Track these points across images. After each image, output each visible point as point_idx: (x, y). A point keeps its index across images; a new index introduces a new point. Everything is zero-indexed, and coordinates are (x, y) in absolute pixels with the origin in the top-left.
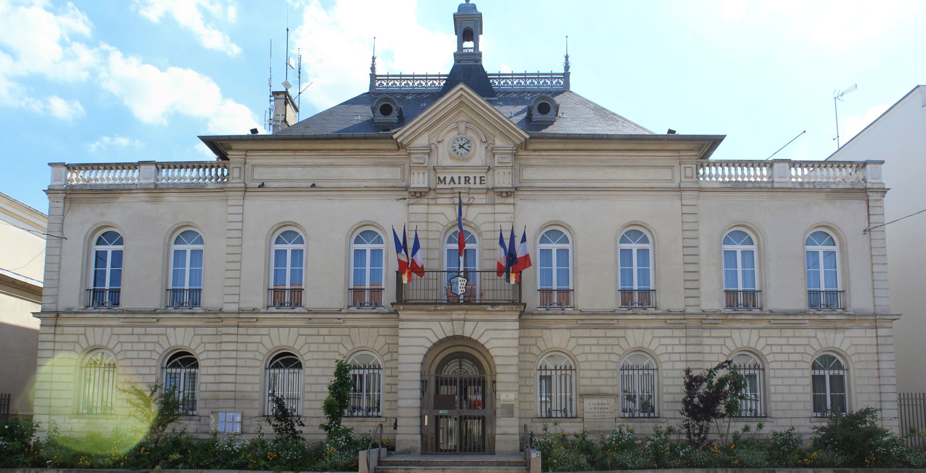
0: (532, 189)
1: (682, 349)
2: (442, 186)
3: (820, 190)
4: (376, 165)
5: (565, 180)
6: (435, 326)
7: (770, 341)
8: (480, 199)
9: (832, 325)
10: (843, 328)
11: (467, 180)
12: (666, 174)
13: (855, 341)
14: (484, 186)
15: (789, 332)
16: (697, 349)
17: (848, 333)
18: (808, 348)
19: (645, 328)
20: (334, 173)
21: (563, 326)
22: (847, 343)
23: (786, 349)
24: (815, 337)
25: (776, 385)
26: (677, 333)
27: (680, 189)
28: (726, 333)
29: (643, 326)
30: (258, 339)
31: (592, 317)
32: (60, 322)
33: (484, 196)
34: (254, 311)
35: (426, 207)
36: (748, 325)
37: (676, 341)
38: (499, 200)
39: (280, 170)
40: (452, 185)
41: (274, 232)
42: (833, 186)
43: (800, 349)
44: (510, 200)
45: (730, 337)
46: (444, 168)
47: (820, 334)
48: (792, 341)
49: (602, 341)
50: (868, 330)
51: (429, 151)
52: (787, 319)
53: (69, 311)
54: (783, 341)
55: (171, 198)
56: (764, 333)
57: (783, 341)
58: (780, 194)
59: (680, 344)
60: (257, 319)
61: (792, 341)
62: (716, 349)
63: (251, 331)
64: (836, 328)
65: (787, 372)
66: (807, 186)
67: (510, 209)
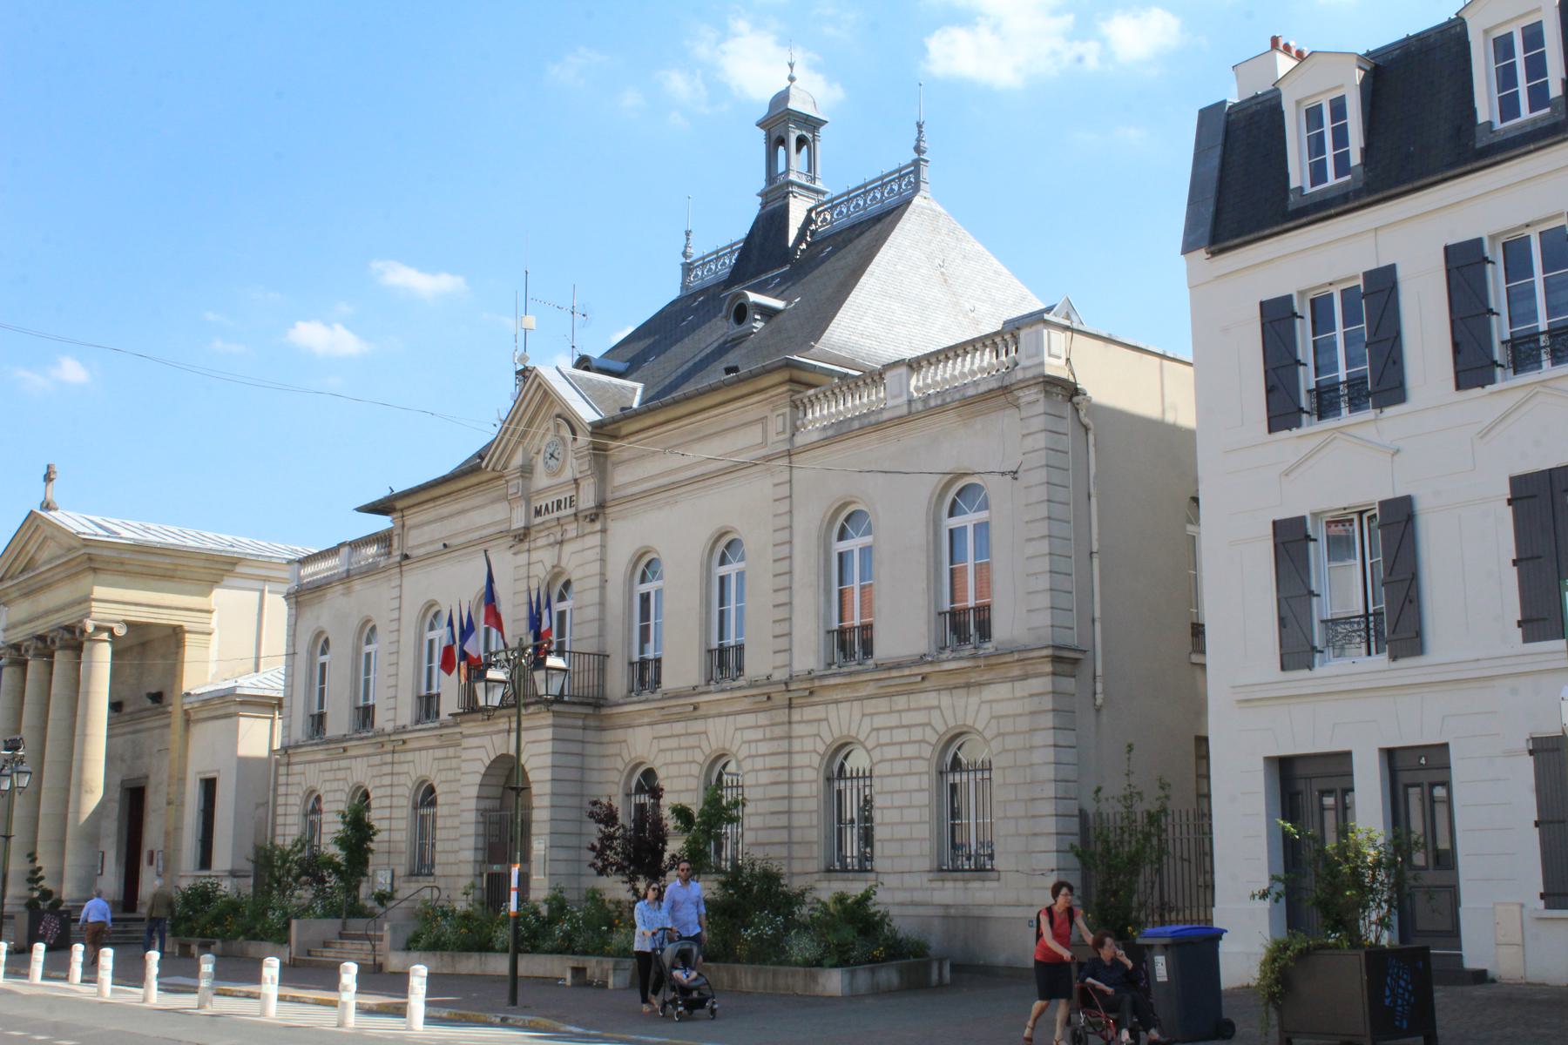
0: (633, 498)
1: (764, 748)
2: (539, 520)
3: (942, 408)
4: (493, 502)
5: (652, 478)
6: (486, 741)
7: (879, 721)
8: (572, 530)
9: (961, 680)
10: (980, 684)
11: (559, 507)
12: (753, 435)
13: (1000, 709)
14: (573, 510)
15: (901, 702)
16: (784, 745)
17: (988, 693)
18: (928, 730)
19: (727, 715)
20: (462, 523)
21: (646, 720)
22: (985, 712)
23: (900, 735)
24: (939, 707)
25: (882, 808)
26: (763, 719)
27: (768, 459)
28: (818, 712)
29: (726, 710)
30: (404, 768)
31: (673, 702)
32: (293, 760)
33: (575, 525)
34: (404, 730)
35: (525, 555)
36: (849, 694)
37: (759, 734)
38: (589, 527)
39: (426, 529)
40: (547, 517)
41: (424, 616)
42: (971, 392)
43: (917, 734)
44: (598, 526)
45: (826, 720)
46: (539, 492)
47: (946, 699)
48: (908, 718)
49: (684, 742)
50: (1017, 684)
51: (527, 471)
52: (911, 675)
53: (297, 746)
54: (893, 720)
55: (358, 585)
56: (870, 706)
57: (893, 720)
58: (893, 431)
59: (764, 740)
60: (404, 742)
61: (908, 718)
62: (808, 744)
63: (403, 757)
64: (968, 686)
65: (897, 780)
66: (932, 403)
67: (595, 540)
